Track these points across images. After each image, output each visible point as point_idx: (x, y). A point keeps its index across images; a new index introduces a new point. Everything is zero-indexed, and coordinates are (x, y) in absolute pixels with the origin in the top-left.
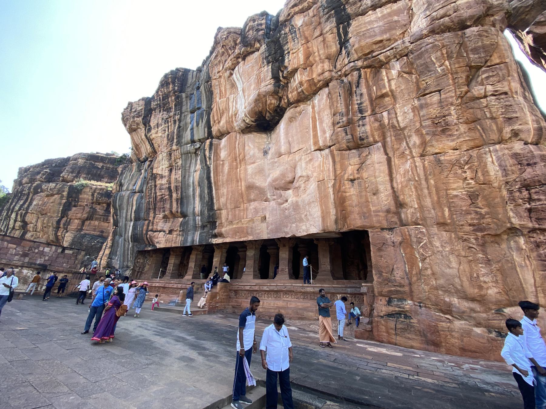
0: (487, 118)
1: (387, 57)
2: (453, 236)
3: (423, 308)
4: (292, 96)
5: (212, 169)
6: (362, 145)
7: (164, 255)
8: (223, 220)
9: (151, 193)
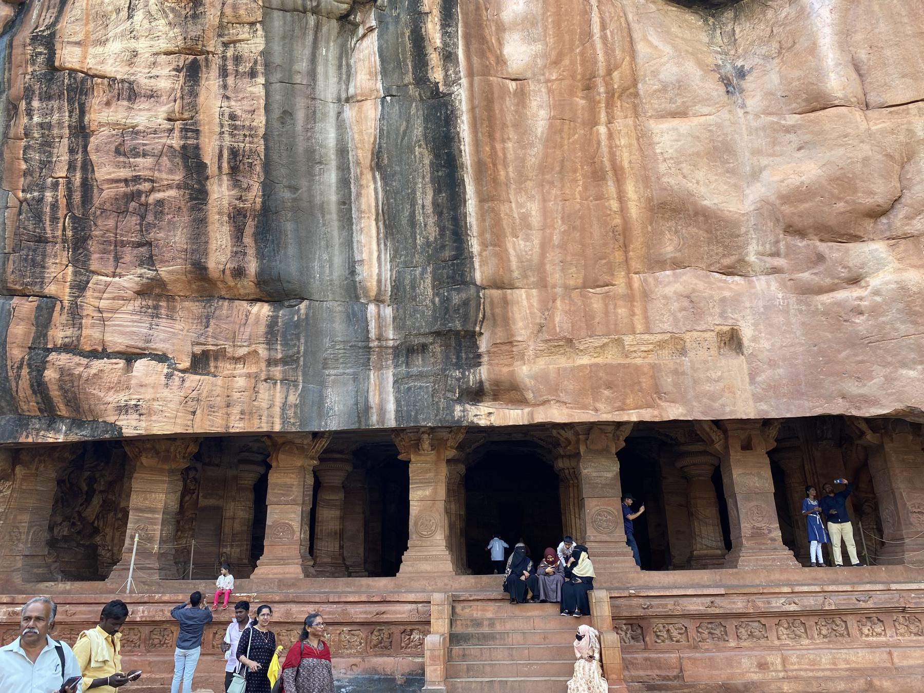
8: (522, 329)
9: (47, 164)
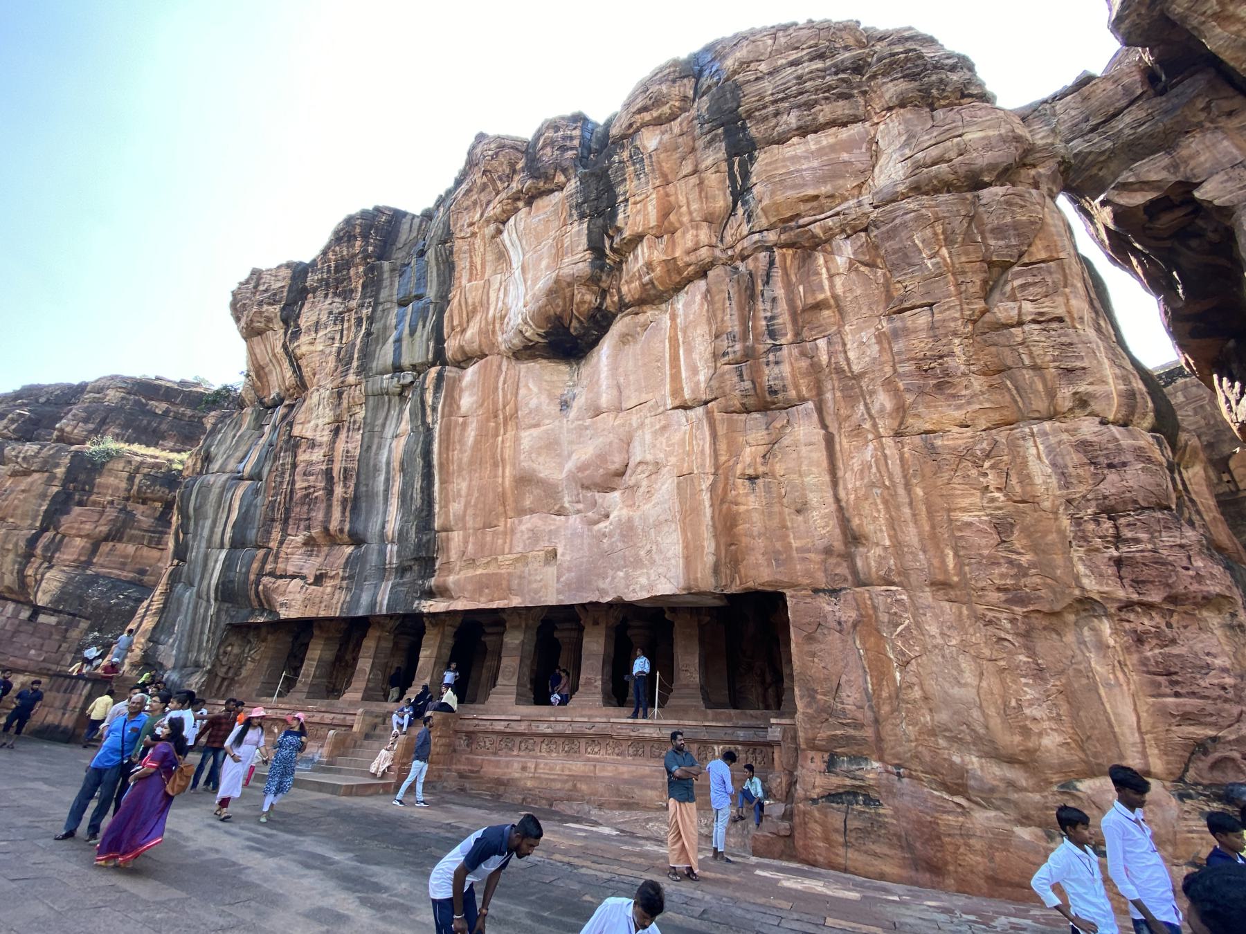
0: (1025, 367)
1: (827, 230)
2: (965, 612)
3: (905, 780)
4: (629, 289)
5: (436, 435)
6: (774, 403)
7: (296, 638)
8: (454, 556)
9: (281, 483)
